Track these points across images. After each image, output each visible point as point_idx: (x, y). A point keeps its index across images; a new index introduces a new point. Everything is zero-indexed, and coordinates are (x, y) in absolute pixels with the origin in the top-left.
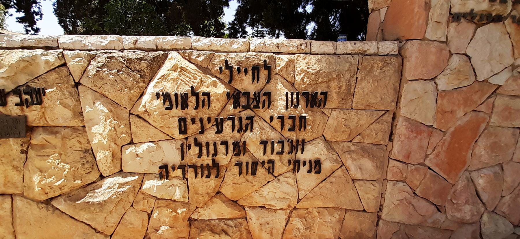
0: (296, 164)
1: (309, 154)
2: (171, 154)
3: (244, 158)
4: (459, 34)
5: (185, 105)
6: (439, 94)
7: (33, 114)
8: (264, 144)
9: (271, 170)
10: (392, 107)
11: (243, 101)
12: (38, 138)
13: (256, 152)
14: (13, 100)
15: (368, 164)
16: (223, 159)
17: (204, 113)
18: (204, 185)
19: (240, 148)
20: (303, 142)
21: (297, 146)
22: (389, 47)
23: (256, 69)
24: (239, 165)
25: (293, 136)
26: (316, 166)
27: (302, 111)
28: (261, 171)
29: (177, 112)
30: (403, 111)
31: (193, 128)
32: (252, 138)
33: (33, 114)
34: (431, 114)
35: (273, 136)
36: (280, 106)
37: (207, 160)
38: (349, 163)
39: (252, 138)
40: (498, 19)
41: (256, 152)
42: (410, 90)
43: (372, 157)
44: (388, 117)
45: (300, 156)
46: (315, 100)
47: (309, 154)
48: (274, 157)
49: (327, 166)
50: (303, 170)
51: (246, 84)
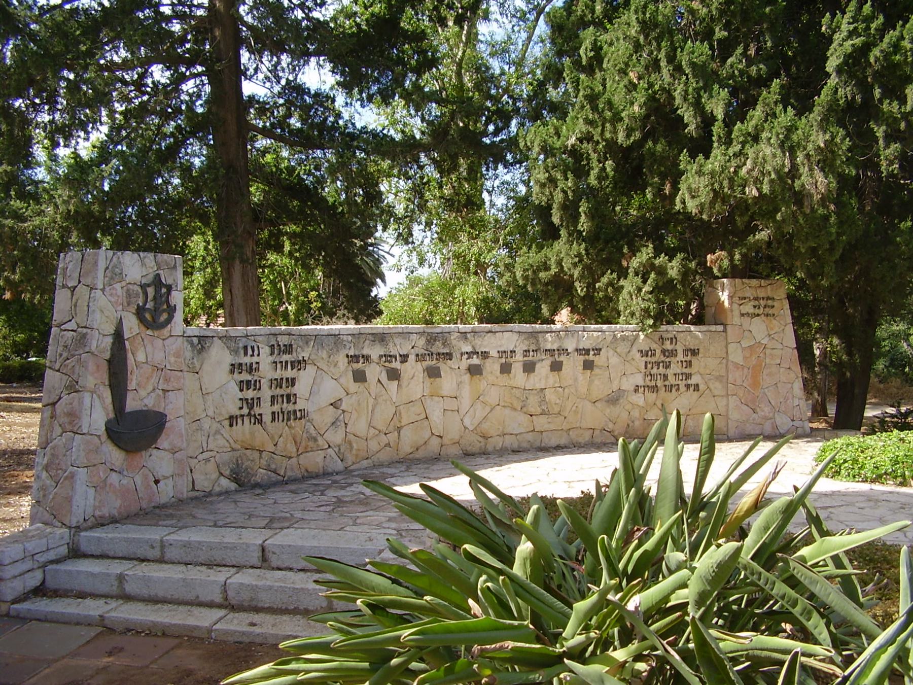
0: (688, 386)
1: (693, 381)
2: (639, 380)
3: (667, 383)
4: (746, 320)
5: (647, 356)
6: (743, 349)
7: (596, 359)
8: (675, 375)
9: (678, 389)
10: (725, 356)
11: (667, 354)
12: (596, 371)
13: (672, 380)
14: (592, 353)
15: (718, 384)
16: (660, 383)
17: (654, 359)
18: (651, 397)
19: (665, 377)
20: (691, 375)
21: (688, 376)
22: (720, 328)
23: (672, 339)
24: (665, 386)
25: (687, 371)
26: (697, 387)
27: (689, 358)
28: (674, 390)
29: (644, 359)
30: (730, 358)
31: (649, 366)
32: (670, 372)
33: (596, 359)
34: (741, 358)
35: (679, 371)
36: (680, 357)
37: (653, 383)
38: (711, 386)
39: (670, 372)
40: (758, 315)
41: (672, 380)
42: (731, 347)
43: (721, 382)
44: (724, 361)
45: (689, 382)
46: (694, 352)
47: (693, 381)
48: (679, 382)
49: (702, 387)
50: (692, 389)
51: (668, 346)
